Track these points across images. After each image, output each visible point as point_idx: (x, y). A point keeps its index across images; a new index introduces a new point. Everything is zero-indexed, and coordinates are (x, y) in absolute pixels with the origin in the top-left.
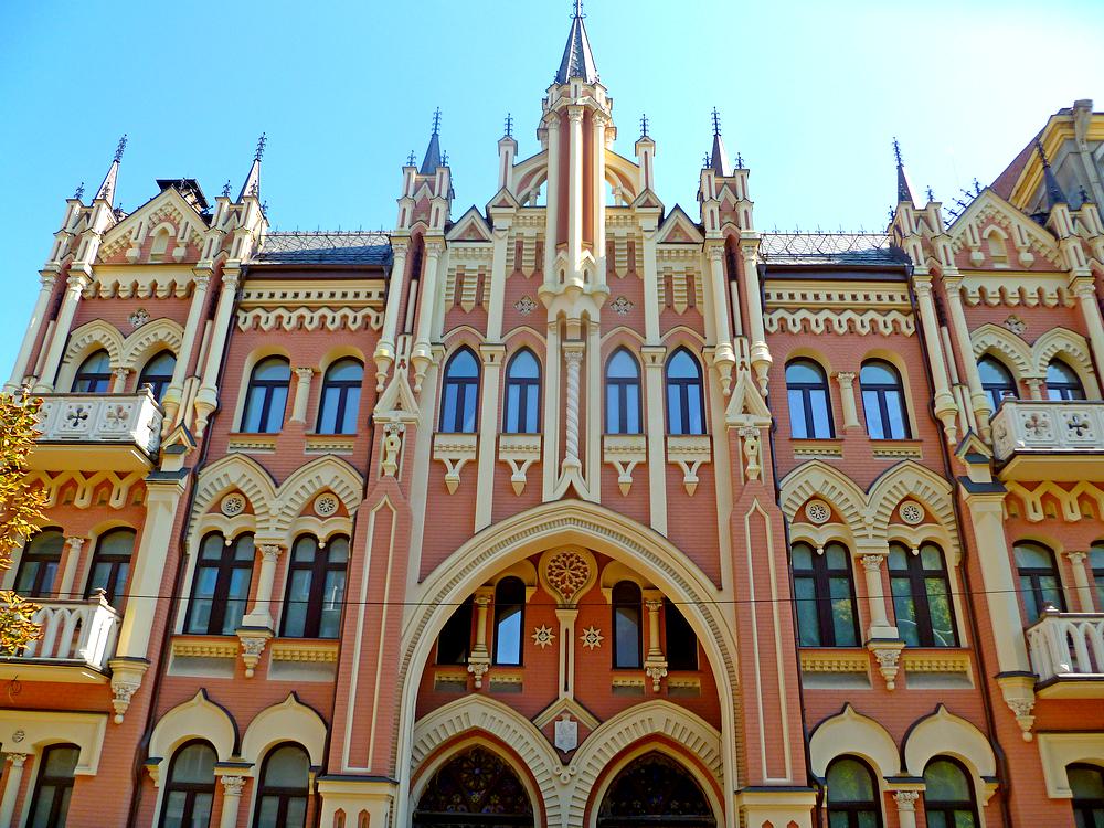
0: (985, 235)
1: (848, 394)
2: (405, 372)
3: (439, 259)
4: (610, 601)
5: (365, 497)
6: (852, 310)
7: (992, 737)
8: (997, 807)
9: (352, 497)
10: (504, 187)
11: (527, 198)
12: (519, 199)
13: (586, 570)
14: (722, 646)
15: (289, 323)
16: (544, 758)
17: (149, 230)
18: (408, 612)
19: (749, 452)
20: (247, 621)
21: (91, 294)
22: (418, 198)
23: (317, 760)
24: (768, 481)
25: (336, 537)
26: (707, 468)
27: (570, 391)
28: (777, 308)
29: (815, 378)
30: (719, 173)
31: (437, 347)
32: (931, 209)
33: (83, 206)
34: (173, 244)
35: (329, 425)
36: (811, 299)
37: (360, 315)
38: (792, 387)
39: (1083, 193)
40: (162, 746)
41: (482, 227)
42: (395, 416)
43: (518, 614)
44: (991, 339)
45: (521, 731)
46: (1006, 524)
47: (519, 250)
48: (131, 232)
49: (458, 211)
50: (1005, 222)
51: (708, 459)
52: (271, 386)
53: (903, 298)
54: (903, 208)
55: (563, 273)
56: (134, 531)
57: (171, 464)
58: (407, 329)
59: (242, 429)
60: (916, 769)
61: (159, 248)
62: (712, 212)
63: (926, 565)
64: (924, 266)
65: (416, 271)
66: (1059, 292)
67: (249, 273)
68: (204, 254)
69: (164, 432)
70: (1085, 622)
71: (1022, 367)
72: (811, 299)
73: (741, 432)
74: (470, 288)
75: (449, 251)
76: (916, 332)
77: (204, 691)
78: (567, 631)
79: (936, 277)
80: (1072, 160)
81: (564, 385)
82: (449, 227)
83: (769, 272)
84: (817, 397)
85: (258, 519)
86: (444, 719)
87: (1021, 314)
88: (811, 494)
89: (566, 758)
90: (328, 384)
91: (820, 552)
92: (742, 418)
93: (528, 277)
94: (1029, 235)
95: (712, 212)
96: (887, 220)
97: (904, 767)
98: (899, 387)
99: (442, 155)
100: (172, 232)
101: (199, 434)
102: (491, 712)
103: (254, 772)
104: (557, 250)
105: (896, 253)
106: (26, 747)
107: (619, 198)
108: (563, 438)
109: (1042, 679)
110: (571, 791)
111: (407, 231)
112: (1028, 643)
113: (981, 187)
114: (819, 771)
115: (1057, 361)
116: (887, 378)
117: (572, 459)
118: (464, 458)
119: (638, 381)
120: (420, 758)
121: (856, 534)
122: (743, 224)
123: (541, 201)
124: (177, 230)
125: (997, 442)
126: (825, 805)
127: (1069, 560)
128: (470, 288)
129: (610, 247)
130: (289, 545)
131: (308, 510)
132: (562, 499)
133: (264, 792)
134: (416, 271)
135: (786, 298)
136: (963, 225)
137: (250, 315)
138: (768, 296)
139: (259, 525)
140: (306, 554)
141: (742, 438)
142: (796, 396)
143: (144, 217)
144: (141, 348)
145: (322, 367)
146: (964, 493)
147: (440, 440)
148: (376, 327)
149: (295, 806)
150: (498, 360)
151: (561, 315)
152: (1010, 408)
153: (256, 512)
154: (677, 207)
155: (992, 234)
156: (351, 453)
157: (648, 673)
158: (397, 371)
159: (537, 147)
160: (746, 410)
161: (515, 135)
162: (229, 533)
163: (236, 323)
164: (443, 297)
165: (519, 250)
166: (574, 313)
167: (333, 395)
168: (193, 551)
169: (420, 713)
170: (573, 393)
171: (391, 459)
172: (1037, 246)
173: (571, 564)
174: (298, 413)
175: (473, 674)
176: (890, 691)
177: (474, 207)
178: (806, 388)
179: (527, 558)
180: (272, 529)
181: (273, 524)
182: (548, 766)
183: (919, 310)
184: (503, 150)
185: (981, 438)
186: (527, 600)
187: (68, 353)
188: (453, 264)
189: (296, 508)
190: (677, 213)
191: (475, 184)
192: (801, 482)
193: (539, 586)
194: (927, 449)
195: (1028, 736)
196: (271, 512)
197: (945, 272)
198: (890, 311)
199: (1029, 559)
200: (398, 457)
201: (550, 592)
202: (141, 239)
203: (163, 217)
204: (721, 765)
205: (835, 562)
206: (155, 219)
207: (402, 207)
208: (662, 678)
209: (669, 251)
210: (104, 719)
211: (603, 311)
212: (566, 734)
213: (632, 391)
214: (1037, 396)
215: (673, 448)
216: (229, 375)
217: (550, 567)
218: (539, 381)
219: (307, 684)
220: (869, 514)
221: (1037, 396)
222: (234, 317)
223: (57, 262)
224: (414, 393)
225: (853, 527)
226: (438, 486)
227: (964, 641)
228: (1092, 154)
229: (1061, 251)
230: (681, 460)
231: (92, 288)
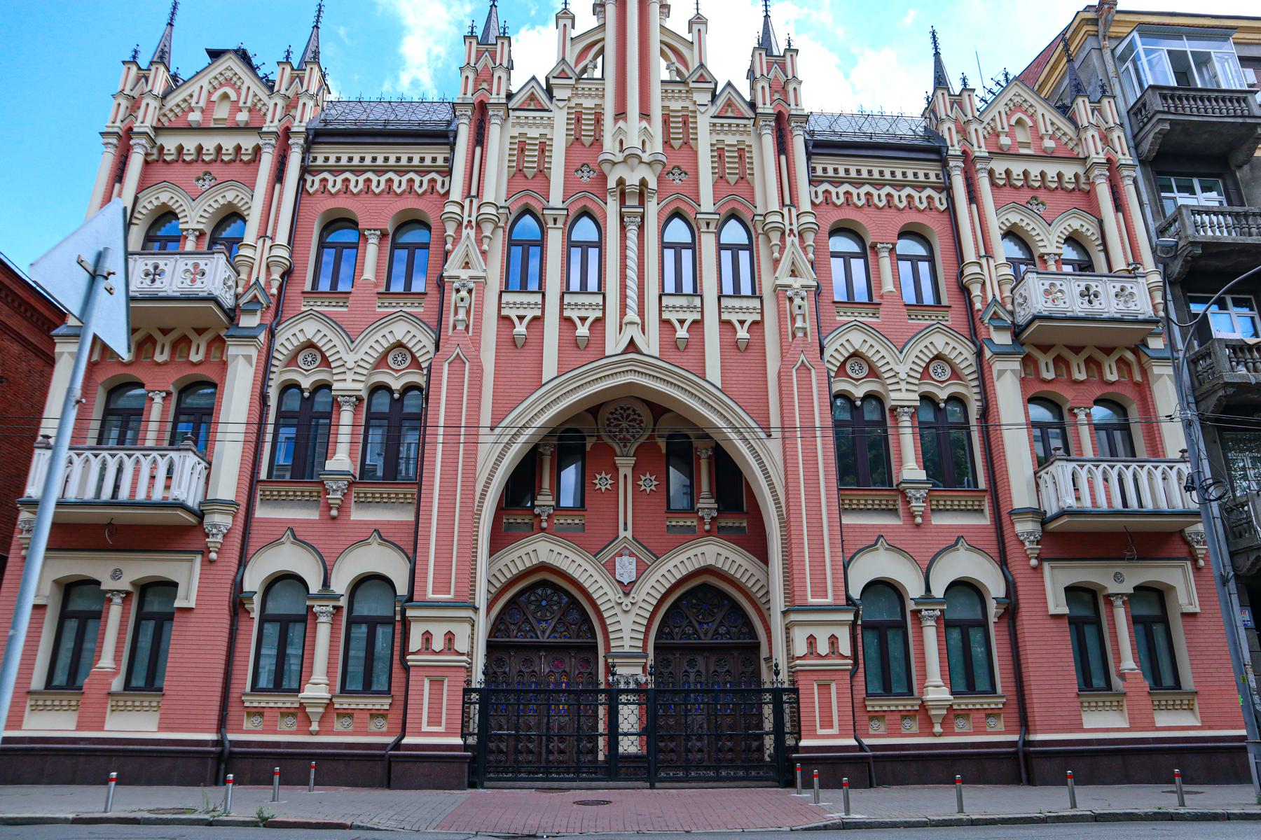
0: (1013, 122)
1: (885, 262)
2: (472, 233)
3: (502, 126)
4: (664, 451)
5: (437, 348)
6: (892, 186)
7: (1003, 562)
8: (1004, 625)
9: (424, 351)
10: (563, 59)
11: (584, 70)
12: (577, 70)
13: (641, 421)
14: (771, 486)
15: (356, 186)
16: (607, 589)
17: (210, 94)
18: (483, 450)
19: (797, 311)
21: (154, 157)
22: (480, 66)
23: (402, 589)
24: (812, 338)
25: (409, 388)
27: (629, 253)
28: (822, 182)
29: (854, 248)
30: (769, 53)
31: (501, 211)
32: (966, 94)
33: (139, 68)
34: (236, 108)
35: (397, 287)
36: (853, 174)
37: (426, 179)
38: (835, 255)
39: (1102, 87)
41: (543, 97)
42: (464, 274)
44: (1015, 218)
45: (585, 565)
46: (1023, 381)
47: (578, 120)
48: (191, 96)
49: (518, 81)
50: (1031, 111)
51: (758, 318)
52: (340, 248)
53: (937, 176)
54: (939, 93)
55: (621, 142)
56: (214, 386)
57: (246, 321)
58: (473, 191)
59: (313, 288)
60: (938, 591)
61: (222, 112)
62: (763, 88)
64: (957, 147)
66: (1076, 176)
67: (319, 136)
68: (269, 118)
69: (240, 290)
70: (1089, 465)
71: (1040, 244)
72: (853, 174)
73: (789, 293)
74: (532, 154)
75: (511, 120)
76: (948, 208)
77: (292, 531)
78: (625, 476)
80: (1094, 54)
81: (624, 248)
82: (510, 96)
83: (819, 147)
84: (857, 265)
85: (335, 371)
86: (514, 556)
87: (1042, 196)
88: (852, 351)
89: (627, 589)
90: (395, 246)
91: (858, 403)
92: (790, 281)
93: (587, 144)
94: (1052, 124)
95: (763, 88)
97: (928, 589)
98: (931, 259)
99: (501, 24)
100: (233, 97)
101: (274, 291)
102: (557, 549)
103: (343, 602)
104: (616, 120)
105: (931, 133)
106: (124, 584)
107: (674, 73)
108: (624, 297)
110: (632, 617)
111: (470, 98)
112: (1037, 485)
113: (1011, 77)
114: (855, 593)
115: (1072, 240)
116: (920, 251)
117: (632, 315)
118: (530, 314)
119: (693, 246)
120: (493, 590)
121: (891, 388)
122: (792, 102)
123: (597, 74)
124: (239, 95)
125: (1018, 309)
126: (859, 622)
127: (1075, 415)
128: (532, 154)
129: (666, 121)
130: (364, 394)
131: (382, 362)
132: (624, 353)
133: (353, 621)
134: (480, 138)
135: (831, 173)
136: (994, 112)
137: (317, 179)
138: (814, 169)
139: (336, 378)
140: (382, 403)
141: (791, 299)
142: (837, 265)
143: (204, 82)
144: (211, 210)
145: (390, 228)
146: (988, 354)
147: (507, 298)
148: (442, 192)
150: (560, 225)
151: (621, 182)
152: (1031, 278)
153: (333, 365)
154: (729, 84)
155: (1019, 122)
156: (421, 310)
157: (700, 514)
158: (464, 232)
159: (593, 22)
160: (793, 273)
161: (571, 8)
162: (306, 383)
163: (304, 186)
164: (506, 164)
165: (578, 120)
166: (633, 179)
167: (402, 254)
168: (273, 402)
169: (493, 551)
170: (632, 254)
171: (462, 315)
172: (1059, 134)
173: (628, 416)
174: (369, 273)
175: (539, 515)
176: (918, 525)
177: (534, 78)
178: (846, 257)
179: (587, 411)
180: (349, 380)
181: (350, 376)
182: (611, 596)
183: (951, 188)
184: (561, 22)
185: (1003, 306)
186: (588, 449)
187: (136, 215)
188: (515, 132)
189: (372, 360)
190: (729, 89)
191: (534, 55)
192: (843, 340)
193: (599, 438)
194: (955, 318)
195: (1034, 562)
197: (977, 154)
198: (925, 188)
199: (1041, 413)
200: (468, 312)
201: (609, 441)
202: (202, 103)
203: (223, 82)
204: (767, 592)
205: (871, 414)
206: (215, 83)
207: (464, 75)
208: (713, 518)
209: (722, 125)
210: (199, 558)
211: (660, 179)
212: (626, 568)
213: (687, 255)
214: (1052, 268)
215: (726, 308)
216: (299, 238)
217: (608, 419)
218: (600, 245)
219: (389, 523)
220: (903, 370)
221: (1052, 268)
222: (302, 179)
223: (118, 124)
224: (484, 253)
225: (889, 382)
226: (509, 343)
227: (982, 484)
228: (1113, 51)
230: (734, 318)
231: (155, 151)
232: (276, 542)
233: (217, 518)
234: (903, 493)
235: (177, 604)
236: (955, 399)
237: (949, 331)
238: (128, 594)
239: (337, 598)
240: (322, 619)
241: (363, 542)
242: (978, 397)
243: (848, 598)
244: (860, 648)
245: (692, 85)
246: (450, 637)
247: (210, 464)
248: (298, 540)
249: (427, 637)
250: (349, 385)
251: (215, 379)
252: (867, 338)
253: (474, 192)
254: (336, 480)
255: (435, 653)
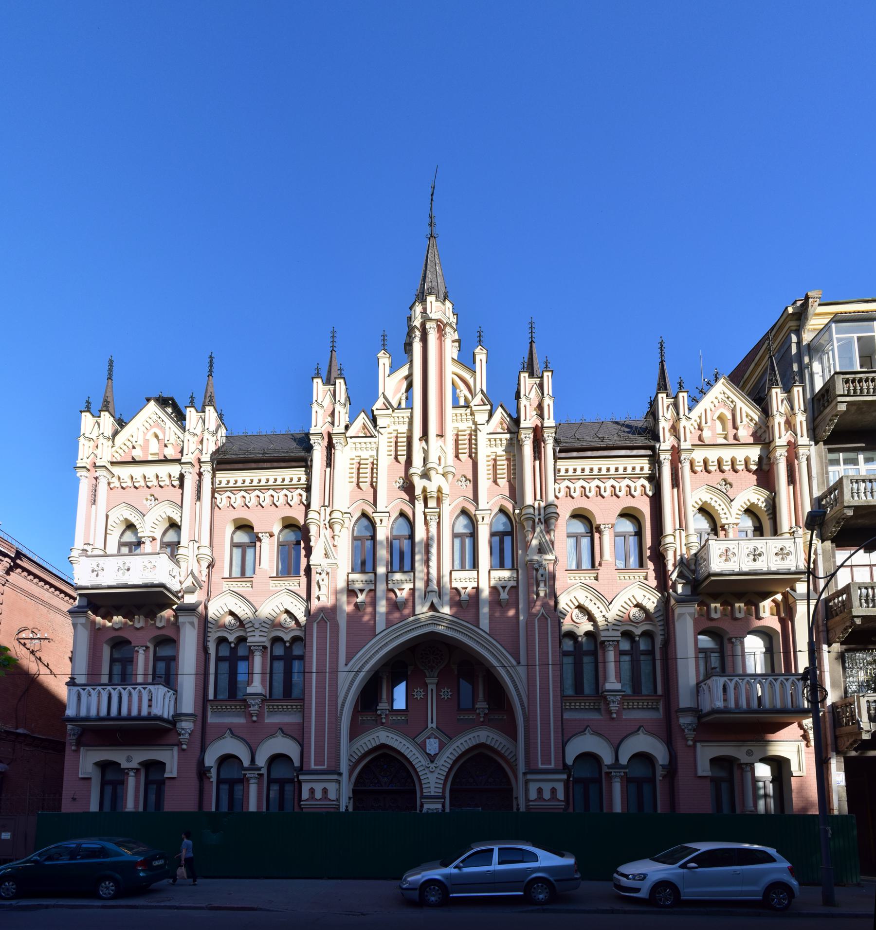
0: (715, 417)
14: (519, 695)
20: (250, 690)
23: (297, 763)
26: (515, 588)
31: (345, 515)
40: (210, 760)
43: (404, 684)
45: (408, 745)
51: (515, 584)
63: (642, 647)
65: (329, 462)
79: (676, 452)
94: (747, 416)
96: (646, 408)
102: (391, 735)
103: (264, 771)
109: (705, 711)
130: (268, 645)
138: (559, 471)
139: (249, 634)
149: (288, 788)
151: (424, 490)
175: (380, 715)
176: (613, 719)
180: (257, 636)
181: (257, 633)
188: (354, 454)
196: (256, 626)
199: (705, 641)
210: (176, 748)
211: (452, 486)
219: (287, 724)
222: (213, 497)
227: (660, 691)
229: (768, 427)
232: (221, 737)
233: (184, 725)
234: (605, 698)
235: (166, 775)
236: (645, 634)
237: (644, 586)
238: (138, 770)
239: (260, 769)
240: (252, 781)
241: (273, 735)
242: (662, 633)
243: (565, 765)
244: (571, 794)
245: (474, 408)
246: (325, 791)
247: (176, 691)
248: (234, 735)
249: (312, 791)
250: (257, 639)
251: (174, 637)
252: (588, 595)
253: (326, 503)
254: (254, 699)
255: (317, 800)
